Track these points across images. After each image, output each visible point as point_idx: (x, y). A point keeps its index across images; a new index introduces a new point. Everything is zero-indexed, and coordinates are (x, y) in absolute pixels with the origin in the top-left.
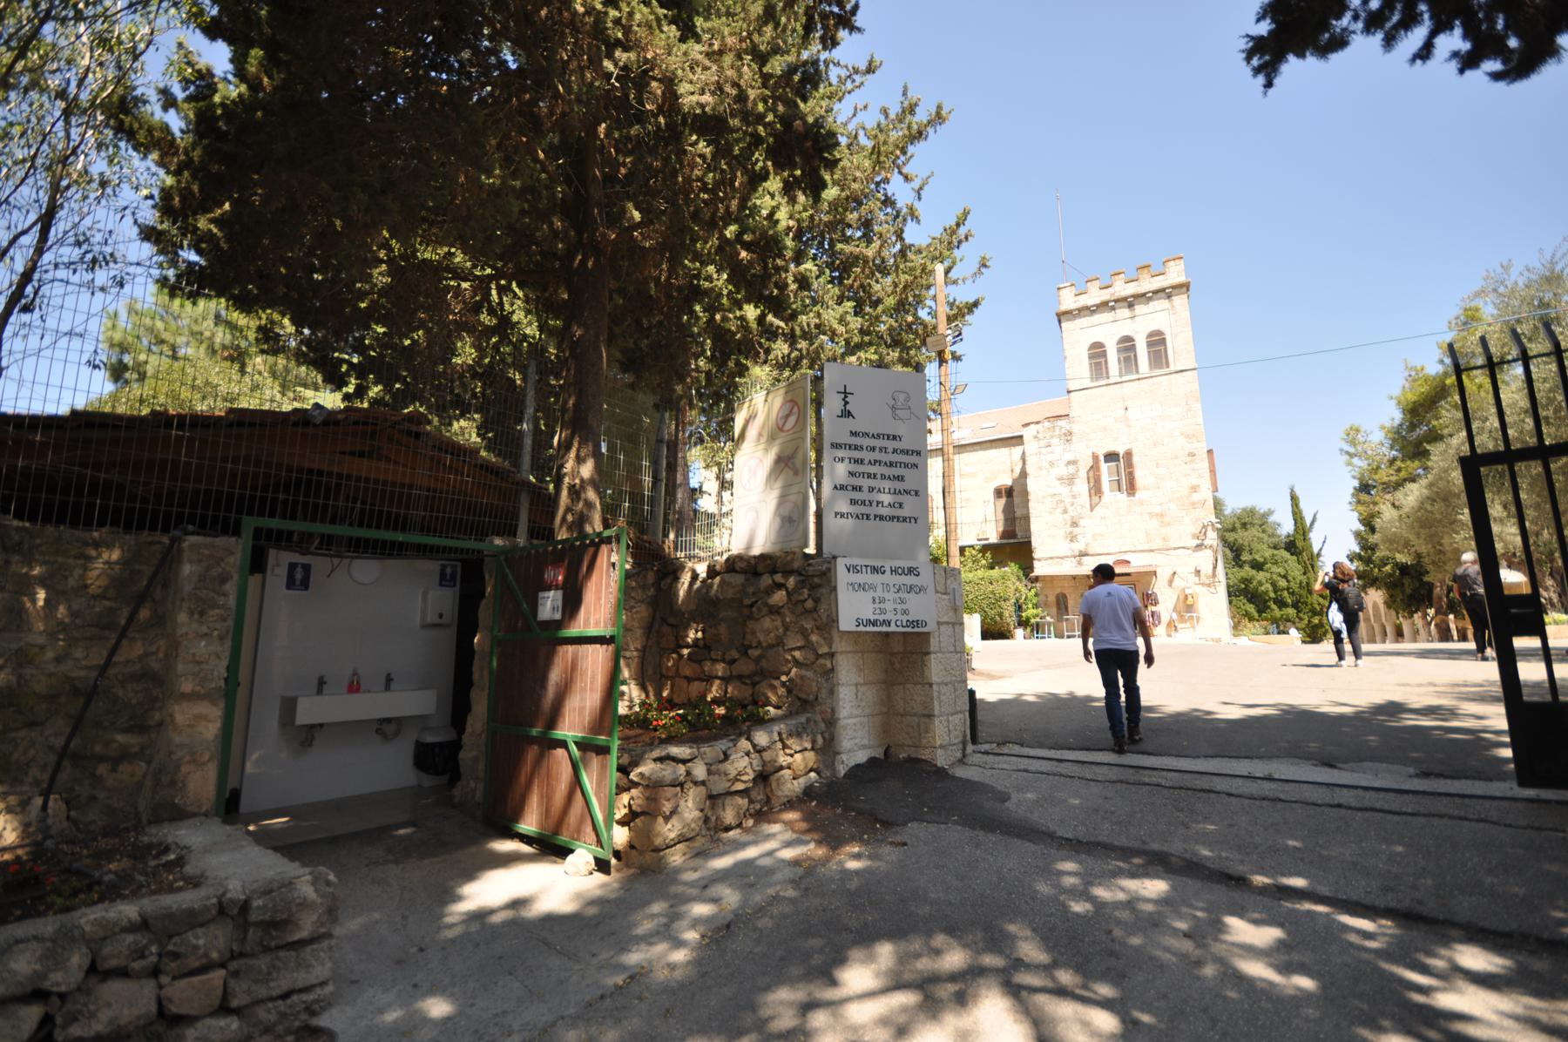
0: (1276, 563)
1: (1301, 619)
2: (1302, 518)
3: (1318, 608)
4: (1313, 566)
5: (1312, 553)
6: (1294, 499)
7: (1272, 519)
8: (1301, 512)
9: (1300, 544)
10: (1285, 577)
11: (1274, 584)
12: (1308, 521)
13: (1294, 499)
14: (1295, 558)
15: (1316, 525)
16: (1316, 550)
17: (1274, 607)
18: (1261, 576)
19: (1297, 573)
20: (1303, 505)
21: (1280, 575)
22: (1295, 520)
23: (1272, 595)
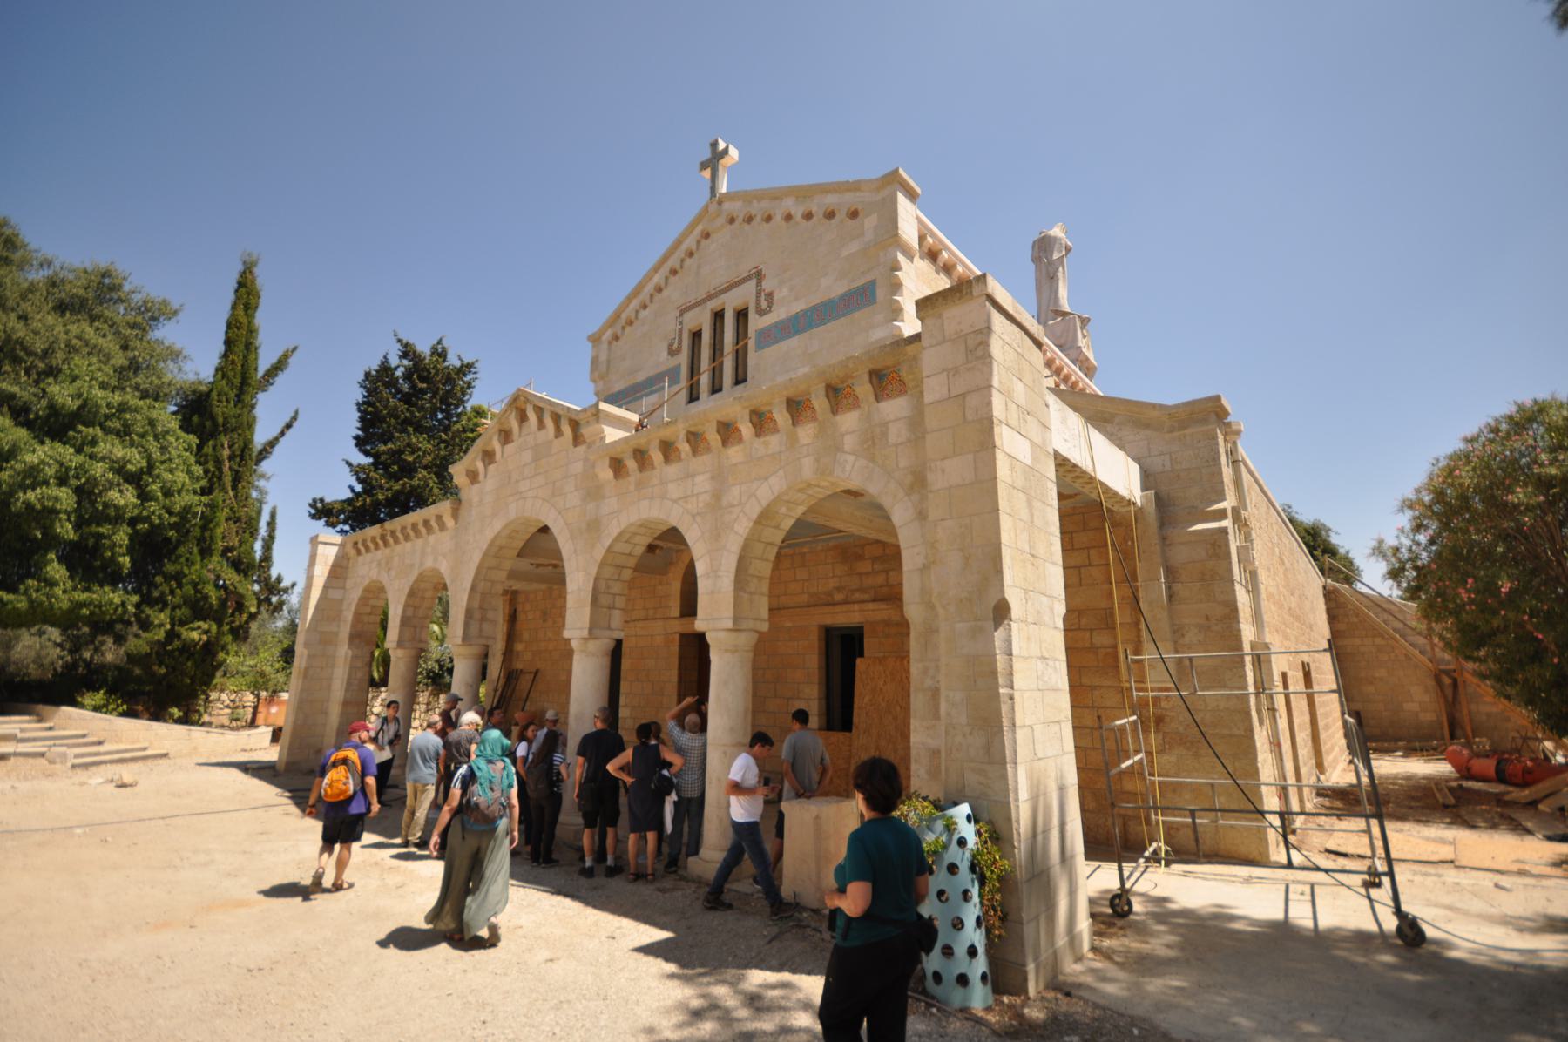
0: (124, 433)
1: (145, 625)
2: (250, 347)
3: (214, 596)
4: (237, 479)
5: (247, 444)
6: (246, 294)
7: (165, 333)
8: (252, 331)
9: (220, 410)
10: (134, 479)
11: (85, 493)
12: (264, 363)
13: (246, 294)
14: (193, 440)
15: (281, 379)
16: (260, 437)
17: (56, 570)
18: (40, 454)
19: (181, 477)
20: (261, 319)
21: (120, 469)
22: (229, 343)
23: (66, 530)
